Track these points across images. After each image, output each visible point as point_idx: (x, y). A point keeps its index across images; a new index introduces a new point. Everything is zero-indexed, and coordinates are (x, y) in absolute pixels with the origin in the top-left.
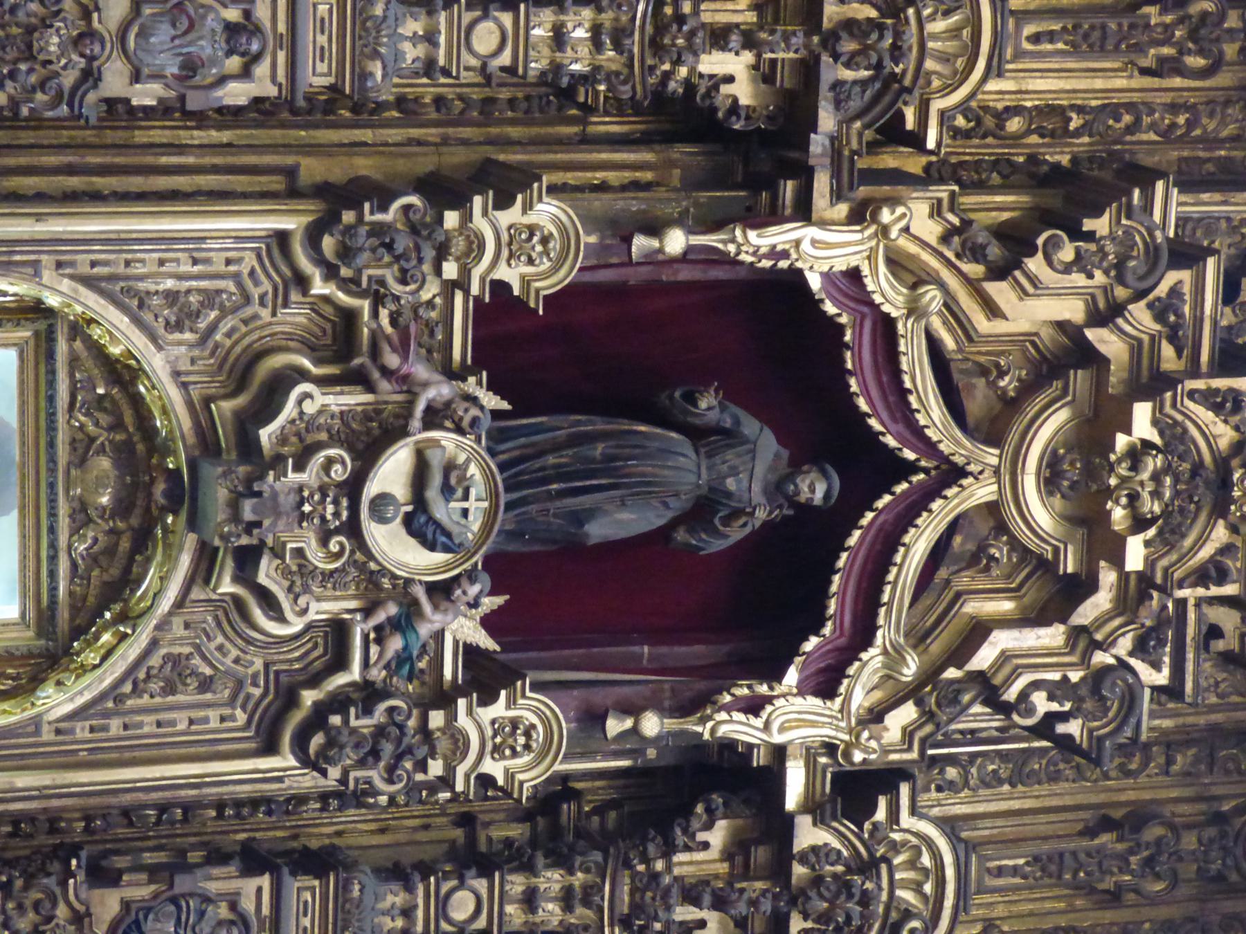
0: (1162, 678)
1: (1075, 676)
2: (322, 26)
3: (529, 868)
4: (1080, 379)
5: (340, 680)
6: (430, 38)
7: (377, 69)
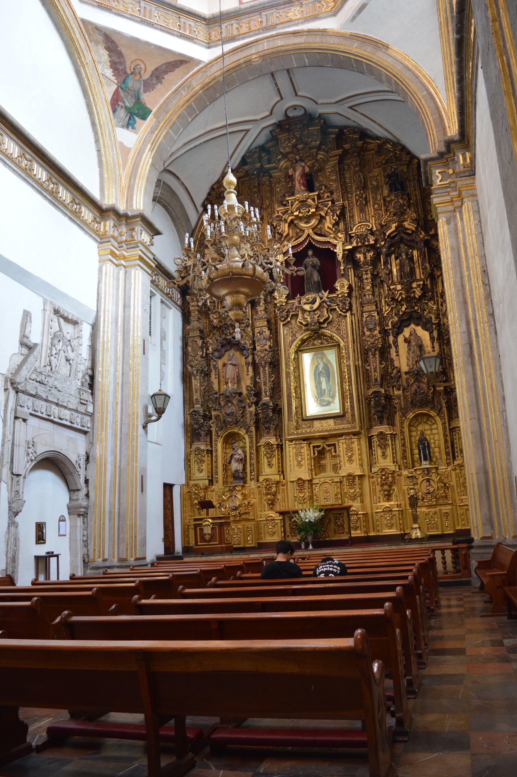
0: (330, 203)
1: (331, 214)
2: (260, 324)
3: (363, 279)
4: (295, 222)
5: (338, 309)
6: (261, 311)
7: (263, 317)
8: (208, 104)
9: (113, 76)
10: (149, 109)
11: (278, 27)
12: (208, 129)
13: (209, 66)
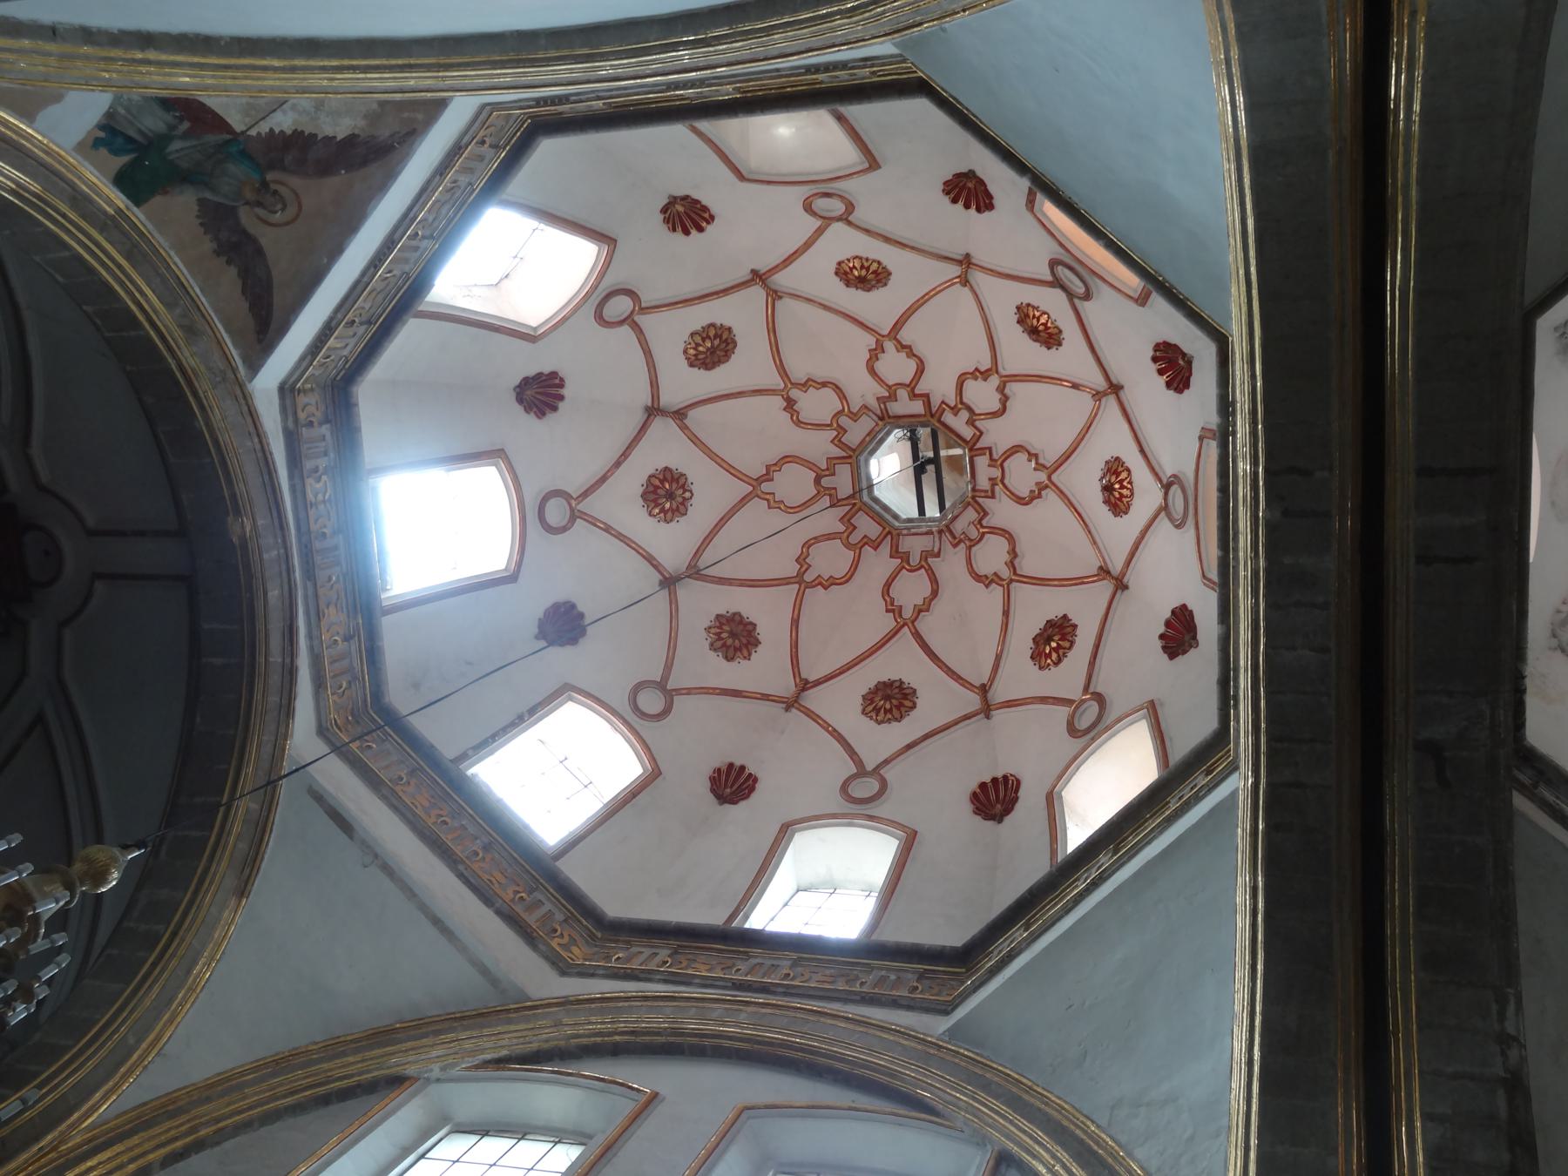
8: (128, 368)
9: (271, 130)
10: (146, 201)
11: (309, 584)
12: (28, 316)
13: (238, 392)
